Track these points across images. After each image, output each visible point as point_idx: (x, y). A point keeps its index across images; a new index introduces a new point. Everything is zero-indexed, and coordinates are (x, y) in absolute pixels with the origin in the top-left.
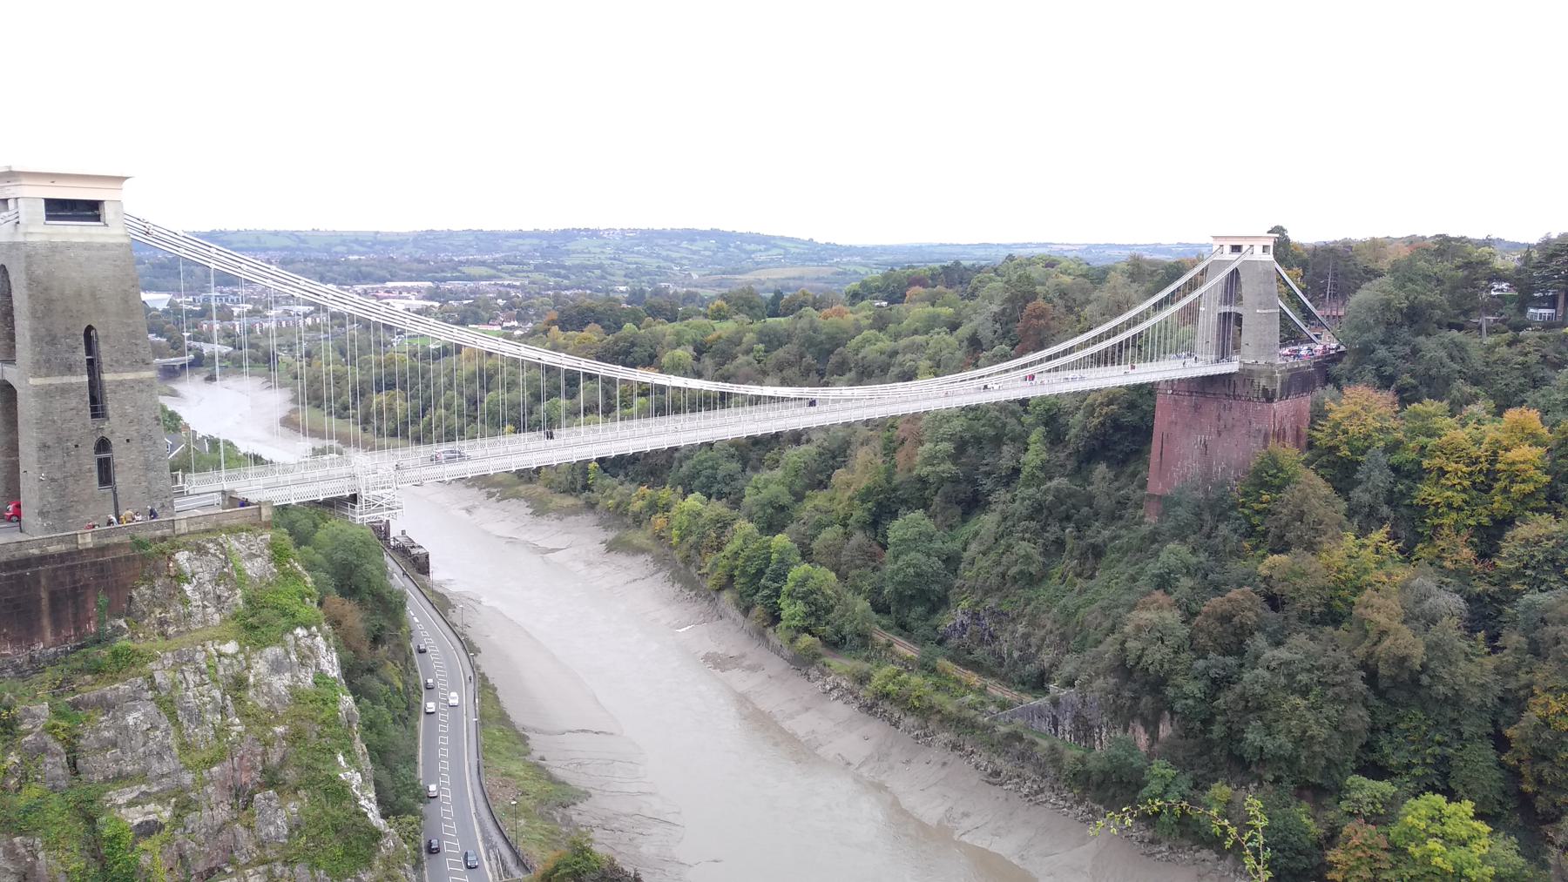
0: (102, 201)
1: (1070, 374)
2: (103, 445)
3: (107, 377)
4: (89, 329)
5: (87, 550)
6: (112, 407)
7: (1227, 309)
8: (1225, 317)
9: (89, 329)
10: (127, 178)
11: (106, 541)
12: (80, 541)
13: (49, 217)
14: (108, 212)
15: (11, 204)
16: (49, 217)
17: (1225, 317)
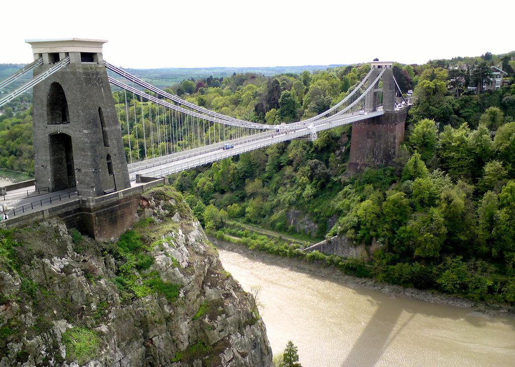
0: (96, 53)
1: (346, 115)
2: (108, 157)
3: (107, 129)
4: (100, 109)
5: (122, 199)
6: (110, 143)
7: (376, 90)
8: (375, 94)
9: (100, 109)
10: (104, 43)
11: (126, 195)
12: (120, 196)
13: (83, 60)
14: (100, 60)
15: (62, 56)
16: (83, 60)
17: (375, 94)
